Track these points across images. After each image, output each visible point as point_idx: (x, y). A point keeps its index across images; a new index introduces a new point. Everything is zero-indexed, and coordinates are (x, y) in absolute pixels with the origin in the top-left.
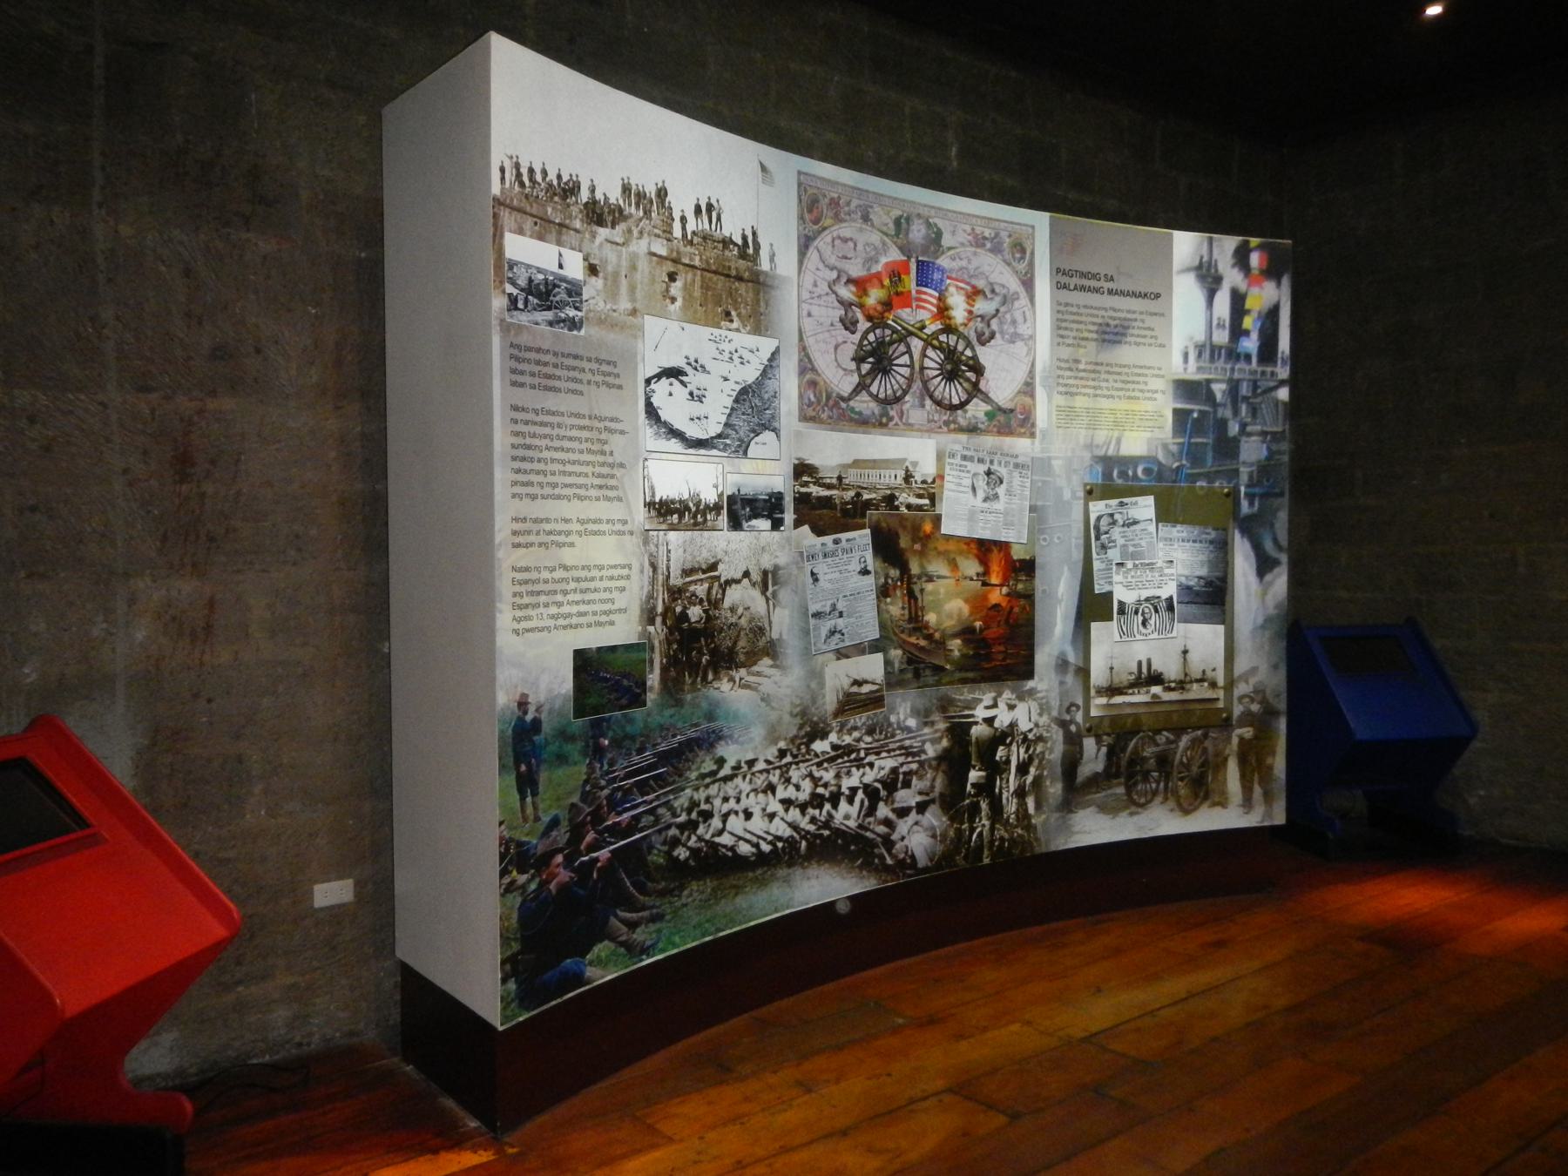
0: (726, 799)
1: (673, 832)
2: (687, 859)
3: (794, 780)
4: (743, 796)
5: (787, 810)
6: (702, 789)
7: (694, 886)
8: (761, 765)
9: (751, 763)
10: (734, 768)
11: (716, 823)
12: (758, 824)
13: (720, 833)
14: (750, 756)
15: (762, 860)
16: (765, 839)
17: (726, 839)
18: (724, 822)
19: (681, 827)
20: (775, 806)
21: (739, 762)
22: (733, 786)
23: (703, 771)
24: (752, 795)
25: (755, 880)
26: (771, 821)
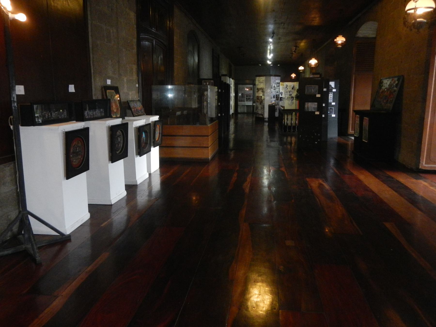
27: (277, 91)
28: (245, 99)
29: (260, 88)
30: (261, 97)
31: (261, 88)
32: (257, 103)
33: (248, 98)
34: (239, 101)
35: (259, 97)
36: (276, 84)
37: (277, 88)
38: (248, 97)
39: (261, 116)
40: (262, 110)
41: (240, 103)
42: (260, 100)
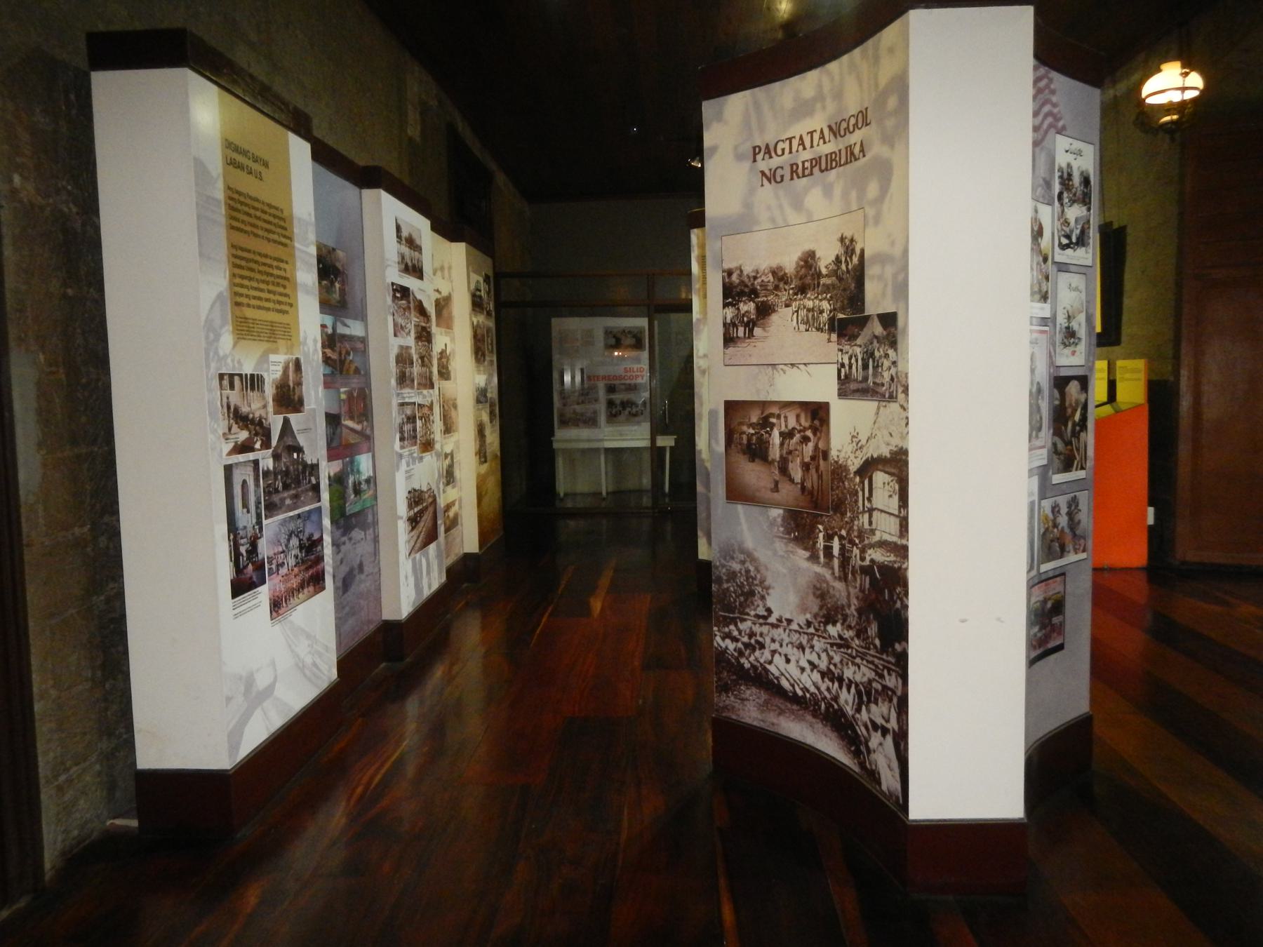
0: (773, 641)
1: (740, 645)
2: (749, 669)
3: (816, 649)
4: (784, 644)
5: (812, 671)
6: (758, 625)
7: (754, 690)
8: (794, 626)
9: (789, 621)
10: (778, 620)
11: (767, 654)
12: (793, 669)
13: (770, 663)
14: (788, 616)
15: (795, 699)
16: (798, 685)
17: (772, 668)
18: (773, 656)
19: (747, 645)
20: (804, 664)
21: (781, 617)
22: (778, 633)
23: (758, 612)
24: (790, 646)
25: (792, 712)
26: (802, 673)
27: (1061, 320)
28: (602, 408)
29: (789, 263)
30: (818, 413)
31: (809, 260)
32: (740, 508)
33: (618, 402)
34: (565, 423)
35: (765, 423)
36: (1050, 203)
37: (1063, 267)
38: (614, 397)
39: (828, 745)
40: (843, 644)
41: (566, 437)
42: (797, 473)
